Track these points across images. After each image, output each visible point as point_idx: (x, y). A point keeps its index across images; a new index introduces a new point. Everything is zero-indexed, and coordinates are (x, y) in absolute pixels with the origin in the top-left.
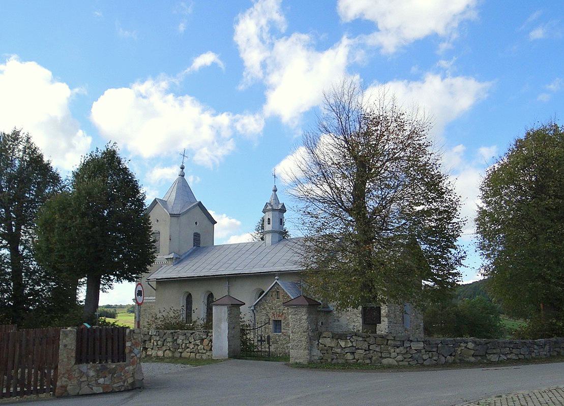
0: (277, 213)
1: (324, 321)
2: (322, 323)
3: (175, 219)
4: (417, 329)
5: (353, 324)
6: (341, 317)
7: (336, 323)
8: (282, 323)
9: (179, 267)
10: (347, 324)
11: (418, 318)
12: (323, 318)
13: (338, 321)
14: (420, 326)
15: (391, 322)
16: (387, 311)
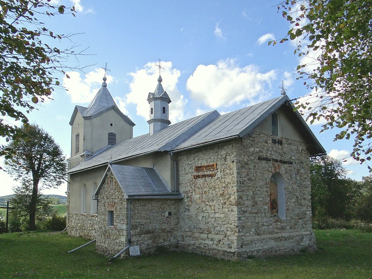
0: (159, 102)
1: (173, 211)
2: (170, 214)
3: (88, 122)
4: (300, 219)
5: (202, 214)
6: (191, 205)
7: (187, 213)
8: (114, 214)
9: (90, 161)
10: (196, 215)
11: (301, 205)
12: (173, 207)
13: (189, 210)
14: (306, 214)
15: (245, 212)
16: (236, 197)
